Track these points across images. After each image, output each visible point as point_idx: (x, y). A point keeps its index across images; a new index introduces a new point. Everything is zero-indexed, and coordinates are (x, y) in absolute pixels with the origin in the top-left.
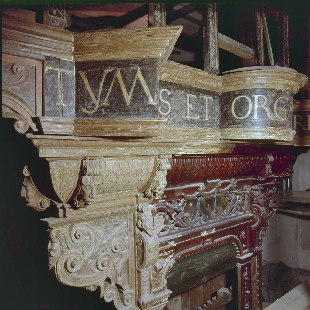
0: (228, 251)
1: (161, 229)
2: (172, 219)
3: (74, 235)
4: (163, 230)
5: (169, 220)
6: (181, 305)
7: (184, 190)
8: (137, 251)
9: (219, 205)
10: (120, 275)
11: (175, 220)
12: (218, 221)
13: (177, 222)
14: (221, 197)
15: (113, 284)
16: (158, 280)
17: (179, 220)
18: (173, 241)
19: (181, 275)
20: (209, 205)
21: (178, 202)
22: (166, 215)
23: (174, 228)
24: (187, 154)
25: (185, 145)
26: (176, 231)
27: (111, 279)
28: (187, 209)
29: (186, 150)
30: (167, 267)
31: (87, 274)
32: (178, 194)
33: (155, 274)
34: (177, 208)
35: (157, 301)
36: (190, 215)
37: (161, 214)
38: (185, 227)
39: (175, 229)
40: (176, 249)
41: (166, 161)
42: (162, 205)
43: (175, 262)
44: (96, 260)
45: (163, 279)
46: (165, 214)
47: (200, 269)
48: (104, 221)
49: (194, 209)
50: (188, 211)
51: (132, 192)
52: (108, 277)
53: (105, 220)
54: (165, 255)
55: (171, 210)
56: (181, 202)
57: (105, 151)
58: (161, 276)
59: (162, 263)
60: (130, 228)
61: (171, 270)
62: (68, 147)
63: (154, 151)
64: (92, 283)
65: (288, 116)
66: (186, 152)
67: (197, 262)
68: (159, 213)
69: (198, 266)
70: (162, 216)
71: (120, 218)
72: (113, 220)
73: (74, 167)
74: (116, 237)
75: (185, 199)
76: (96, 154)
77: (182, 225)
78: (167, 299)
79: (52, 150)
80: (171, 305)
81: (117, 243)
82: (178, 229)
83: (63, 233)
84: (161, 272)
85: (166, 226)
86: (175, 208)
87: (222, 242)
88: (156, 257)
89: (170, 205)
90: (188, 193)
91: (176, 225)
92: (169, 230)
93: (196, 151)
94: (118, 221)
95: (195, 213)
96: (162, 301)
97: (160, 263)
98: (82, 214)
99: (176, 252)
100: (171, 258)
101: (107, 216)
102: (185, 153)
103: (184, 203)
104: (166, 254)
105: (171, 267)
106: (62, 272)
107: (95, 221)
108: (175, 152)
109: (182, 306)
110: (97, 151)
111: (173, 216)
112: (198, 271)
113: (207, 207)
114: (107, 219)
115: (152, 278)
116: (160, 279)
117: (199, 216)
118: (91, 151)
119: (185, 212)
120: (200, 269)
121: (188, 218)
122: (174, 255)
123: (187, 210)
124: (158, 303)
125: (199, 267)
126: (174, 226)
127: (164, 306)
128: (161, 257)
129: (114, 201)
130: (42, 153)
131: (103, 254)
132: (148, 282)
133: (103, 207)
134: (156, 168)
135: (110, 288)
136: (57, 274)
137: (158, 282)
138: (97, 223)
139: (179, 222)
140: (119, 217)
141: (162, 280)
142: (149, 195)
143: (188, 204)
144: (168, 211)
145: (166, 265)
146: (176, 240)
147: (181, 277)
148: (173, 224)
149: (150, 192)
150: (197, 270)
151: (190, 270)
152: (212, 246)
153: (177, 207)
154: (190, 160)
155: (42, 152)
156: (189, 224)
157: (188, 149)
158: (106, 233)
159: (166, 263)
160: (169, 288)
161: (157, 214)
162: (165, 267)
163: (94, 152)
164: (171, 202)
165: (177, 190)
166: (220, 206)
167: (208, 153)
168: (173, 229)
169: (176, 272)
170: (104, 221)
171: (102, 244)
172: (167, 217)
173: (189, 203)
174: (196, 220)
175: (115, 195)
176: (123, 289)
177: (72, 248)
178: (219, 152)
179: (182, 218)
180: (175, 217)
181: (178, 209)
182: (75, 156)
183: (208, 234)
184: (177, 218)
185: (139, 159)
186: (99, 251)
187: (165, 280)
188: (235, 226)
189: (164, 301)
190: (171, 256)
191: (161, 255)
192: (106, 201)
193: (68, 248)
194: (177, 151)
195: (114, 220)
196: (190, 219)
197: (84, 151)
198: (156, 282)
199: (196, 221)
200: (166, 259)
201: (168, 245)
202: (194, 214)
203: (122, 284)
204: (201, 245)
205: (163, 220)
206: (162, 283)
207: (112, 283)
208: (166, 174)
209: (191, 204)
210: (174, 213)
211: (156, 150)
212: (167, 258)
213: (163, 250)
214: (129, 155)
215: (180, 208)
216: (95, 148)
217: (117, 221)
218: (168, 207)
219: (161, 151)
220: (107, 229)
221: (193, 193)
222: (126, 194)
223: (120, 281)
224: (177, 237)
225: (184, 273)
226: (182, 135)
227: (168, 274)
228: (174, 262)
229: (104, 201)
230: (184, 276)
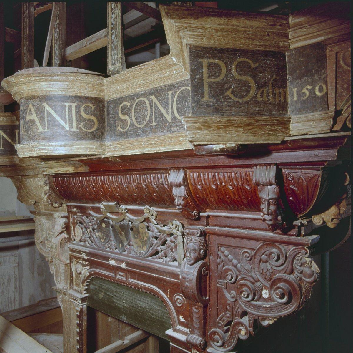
0: (159, 310)
9: (137, 238)
12: (133, 257)
14: (140, 229)
18: (85, 254)
20: (123, 233)
49: (107, 231)
50: (101, 232)
65: (25, 128)
67: (116, 292)
87: (138, 288)
112: (116, 303)
113: (121, 233)
151: (108, 295)
152: (124, 283)
166: (138, 240)
167: (64, 172)
169: (96, 287)
173: (102, 224)
178: (73, 171)
183: (116, 265)
188: (155, 275)
196: (103, 241)
202: (106, 237)
209: (104, 225)
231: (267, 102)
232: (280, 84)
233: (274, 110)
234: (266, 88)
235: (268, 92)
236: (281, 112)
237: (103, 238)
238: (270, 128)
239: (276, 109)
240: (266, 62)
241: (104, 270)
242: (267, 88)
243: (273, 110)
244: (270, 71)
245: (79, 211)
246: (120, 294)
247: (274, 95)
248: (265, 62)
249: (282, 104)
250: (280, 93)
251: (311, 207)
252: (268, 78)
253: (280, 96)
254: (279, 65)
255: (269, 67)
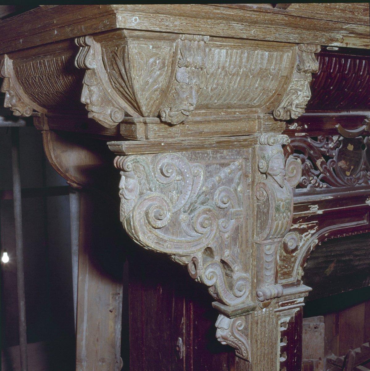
1: (296, 183)
2: (316, 168)
3: (159, 171)
4: (300, 186)
5: (312, 169)
6: (323, 335)
7: (339, 120)
8: (257, 212)
10: (228, 247)
11: (322, 171)
13: (325, 174)
15: (217, 259)
16: (289, 267)
17: (329, 171)
18: (317, 206)
19: (327, 267)
21: (327, 141)
22: (306, 160)
23: (319, 184)
24: (348, 46)
25: (345, 29)
26: (323, 189)
27: (214, 249)
28: (342, 154)
29: (347, 40)
30: (305, 249)
31: (177, 236)
32: (328, 126)
33: (285, 256)
34: (325, 150)
35: (285, 300)
36: (348, 166)
37: (299, 157)
38: (339, 185)
39: (321, 186)
40: (322, 220)
41: (310, 56)
42: (300, 141)
43: (319, 242)
44: (191, 216)
45: (298, 267)
46: (306, 157)
47: (361, 262)
48: (206, 155)
50: (344, 159)
51: (252, 111)
52: (209, 246)
53: (207, 154)
54: (302, 227)
55: (315, 152)
56: (333, 141)
57: (212, 26)
58: (294, 262)
59: (297, 239)
60: (246, 172)
61: (311, 256)
62: (158, 13)
63: (292, 35)
64: (185, 251)
66: (347, 44)
67: (357, 250)
68: (295, 154)
69: (358, 258)
70: (299, 160)
71: (230, 154)
72: (219, 155)
73: (163, 53)
74: (223, 184)
75: (340, 135)
76: (199, 30)
77: (333, 181)
78: (302, 300)
79: (134, 18)
80: (306, 333)
81: (223, 194)
82: (327, 187)
83: (143, 164)
84: (294, 254)
85: (305, 179)
86: (323, 149)
88: (288, 223)
89: (313, 143)
90: (344, 126)
91: (324, 180)
92: (311, 187)
93: (365, 44)
94: (227, 157)
95: (357, 164)
96: (294, 302)
97: (293, 239)
98: (172, 137)
99: (321, 225)
100: (313, 235)
101: (211, 146)
102: (345, 46)
103: (338, 144)
104: (304, 226)
105: (312, 249)
106: (141, 226)
107: (191, 153)
108: (328, 41)
109: (325, 349)
110: (202, 26)
111: (319, 162)
112: (357, 266)
114: (209, 151)
115: (279, 261)
116: (292, 265)
117: (363, 170)
118: (192, 24)
119: (339, 159)
120: (361, 262)
121: (344, 171)
122: (317, 231)
123: (342, 156)
124: (287, 303)
125: (359, 260)
126: (318, 180)
127: (298, 311)
128: (295, 230)
129: (221, 124)
130: (121, 21)
131: (203, 207)
132: (273, 265)
133: (203, 131)
134: (293, 67)
135: (212, 264)
136: (134, 227)
137: (289, 270)
138: (193, 157)
139: (328, 174)
140: (229, 152)
141: (296, 268)
142: (279, 116)
143: (345, 146)
144: (310, 154)
145: (304, 245)
146: (321, 204)
147: (329, 271)
148: (318, 176)
149: (282, 111)
150: (357, 263)
153: (325, 148)
154: (352, 63)
155: (120, 19)
156: (346, 181)
157: (350, 38)
158: (208, 174)
159: (303, 240)
160: (306, 284)
161: (291, 156)
162: (302, 247)
163: (197, 26)
164: (315, 139)
165: (328, 117)
168: (317, 185)
169: (320, 260)
170: (206, 155)
171: (201, 191)
172: (308, 162)
173: (348, 145)
174: (359, 175)
175: (223, 113)
176: (232, 271)
177: (155, 190)
179: (334, 169)
180: (321, 165)
181: (328, 152)
182: (168, 31)
184: (326, 168)
185: (265, 50)
186: (196, 202)
187: (300, 268)
189: (298, 302)
190: (313, 231)
191: (296, 226)
192: (209, 122)
193: (150, 189)
194: (331, 40)
195: (220, 155)
196: (348, 173)
197: (181, 23)
198: (286, 270)
199: (359, 179)
200: (304, 235)
201: (307, 210)
203: (230, 261)
204: (365, 221)
205: (302, 167)
206: (294, 273)
207: (216, 257)
208: (310, 79)
209: (350, 147)
210: (320, 158)
211: (294, 34)
212: (306, 234)
213: (300, 218)
214: (251, 38)
215: (330, 151)
216: (199, 20)
217: (225, 158)
218: (311, 147)
219: (303, 37)
220: (210, 169)
221: (355, 126)
222: (241, 114)
223: (227, 254)
224: (323, 199)
225: (332, 265)
226: (341, 10)
227: (305, 260)
228: (317, 241)
229: (206, 121)
230: (332, 269)
237: (350, 168)
241: (348, 222)
245: (306, 126)
246: (364, 249)
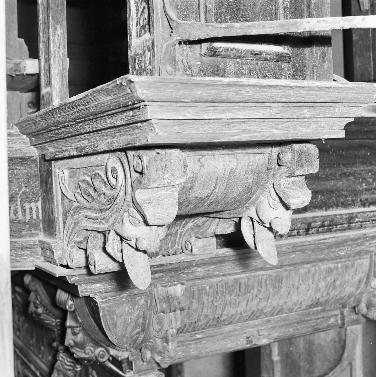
231: (15, 220)
232: (31, 197)
233: (24, 230)
234: (13, 204)
235: (16, 208)
236: (33, 232)
238: (15, 254)
239: (27, 228)
240: (13, 171)
242: (15, 204)
243: (23, 230)
244: (18, 183)
247: (24, 211)
248: (12, 172)
249: (34, 221)
250: (31, 208)
251: (104, 326)
252: (15, 191)
253: (31, 212)
254: (29, 174)
255: (17, 177)
